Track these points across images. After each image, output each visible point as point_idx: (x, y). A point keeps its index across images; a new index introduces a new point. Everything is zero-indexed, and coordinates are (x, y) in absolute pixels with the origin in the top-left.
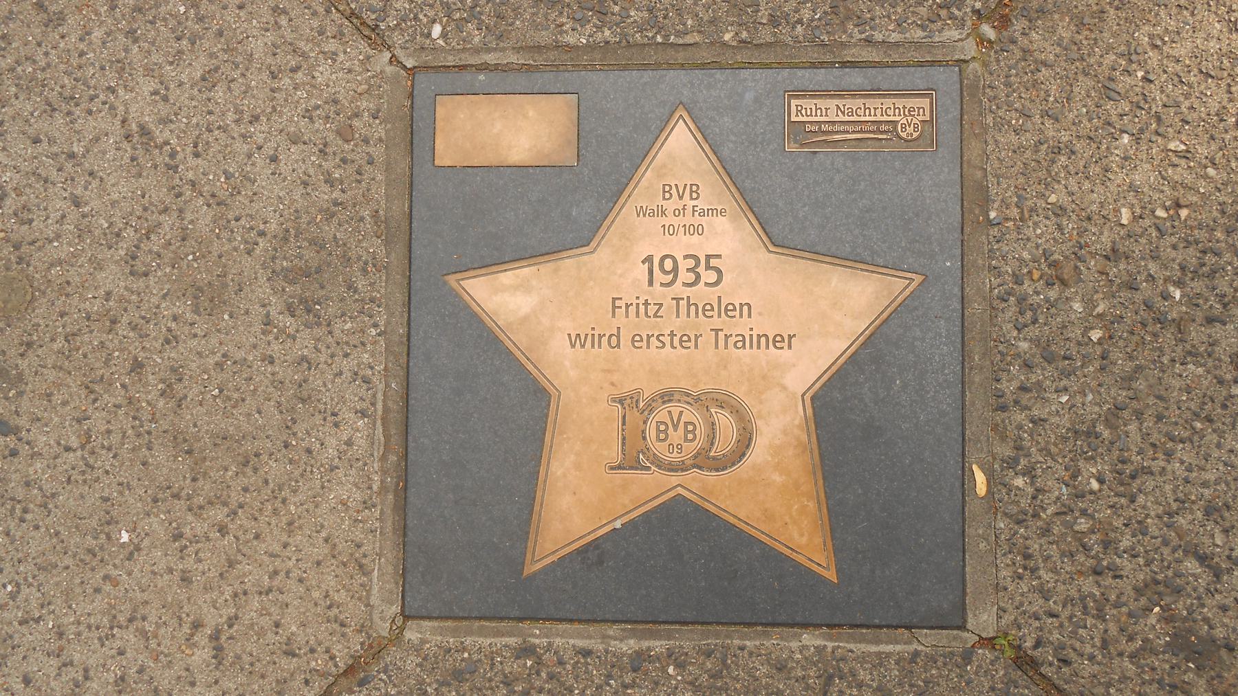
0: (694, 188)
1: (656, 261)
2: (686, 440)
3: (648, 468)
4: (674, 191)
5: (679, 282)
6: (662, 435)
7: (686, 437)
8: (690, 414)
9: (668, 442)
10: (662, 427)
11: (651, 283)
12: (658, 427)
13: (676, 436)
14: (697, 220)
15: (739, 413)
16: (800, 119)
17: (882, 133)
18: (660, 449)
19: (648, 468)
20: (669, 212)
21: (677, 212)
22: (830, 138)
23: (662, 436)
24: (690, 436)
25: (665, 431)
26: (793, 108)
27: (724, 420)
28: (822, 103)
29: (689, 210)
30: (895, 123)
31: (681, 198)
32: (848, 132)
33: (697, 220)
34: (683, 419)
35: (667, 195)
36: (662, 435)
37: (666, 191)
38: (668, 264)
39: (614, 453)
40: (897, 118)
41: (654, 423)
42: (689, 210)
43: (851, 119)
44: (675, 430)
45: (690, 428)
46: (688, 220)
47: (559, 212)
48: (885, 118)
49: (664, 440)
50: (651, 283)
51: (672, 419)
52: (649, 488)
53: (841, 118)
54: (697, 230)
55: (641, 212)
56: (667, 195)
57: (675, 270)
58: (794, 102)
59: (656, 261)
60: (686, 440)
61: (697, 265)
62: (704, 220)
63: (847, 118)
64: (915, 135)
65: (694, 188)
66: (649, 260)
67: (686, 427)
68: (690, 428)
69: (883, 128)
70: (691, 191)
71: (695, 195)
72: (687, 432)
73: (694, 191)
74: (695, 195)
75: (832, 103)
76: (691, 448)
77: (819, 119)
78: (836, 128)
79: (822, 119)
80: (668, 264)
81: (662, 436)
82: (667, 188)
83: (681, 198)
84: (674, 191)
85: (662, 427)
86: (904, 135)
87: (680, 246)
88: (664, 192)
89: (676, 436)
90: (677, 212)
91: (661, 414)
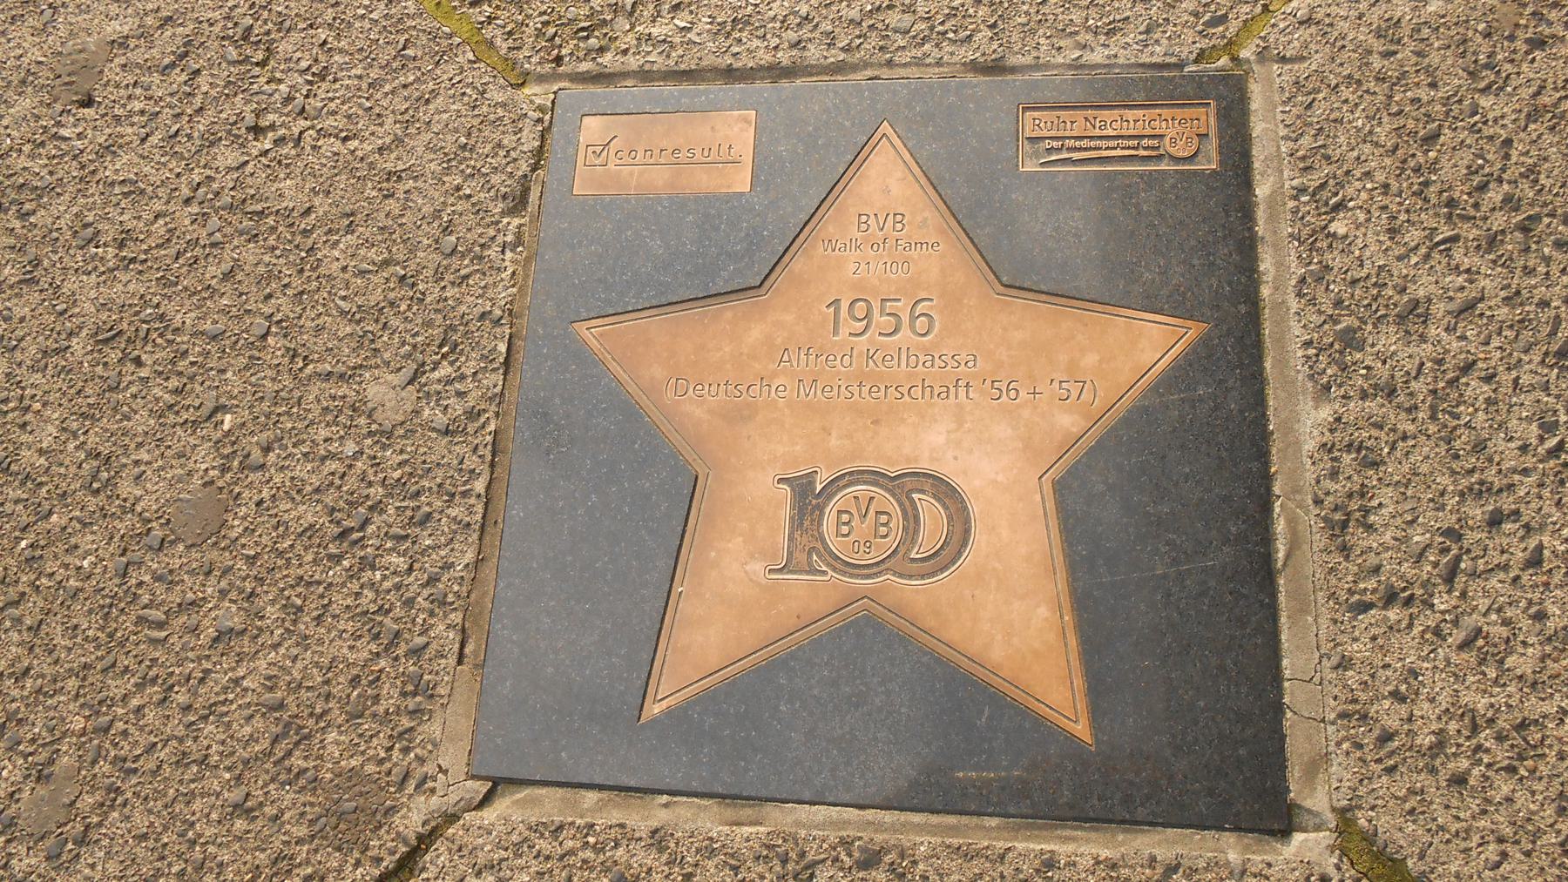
1: (845, 305)
3: (825, 573)
9: (852, 538)
13: (862, 528)
15: (945, 491)
19: (825, 573)
22: (1076, 156)
23: (845, 529)
27: (930, 509)
29: (891, 242)
43: (1105, 133)
51: (859, 509)
59: (845, 305)
63: (1097, 132)
69: (1145, 142)
74: (899, 226)
77: (1060, 134)
78: (1085, 143)
79: (1067, 133)
81: (845, 529)
85: (845, 517)
89: (862, 528)
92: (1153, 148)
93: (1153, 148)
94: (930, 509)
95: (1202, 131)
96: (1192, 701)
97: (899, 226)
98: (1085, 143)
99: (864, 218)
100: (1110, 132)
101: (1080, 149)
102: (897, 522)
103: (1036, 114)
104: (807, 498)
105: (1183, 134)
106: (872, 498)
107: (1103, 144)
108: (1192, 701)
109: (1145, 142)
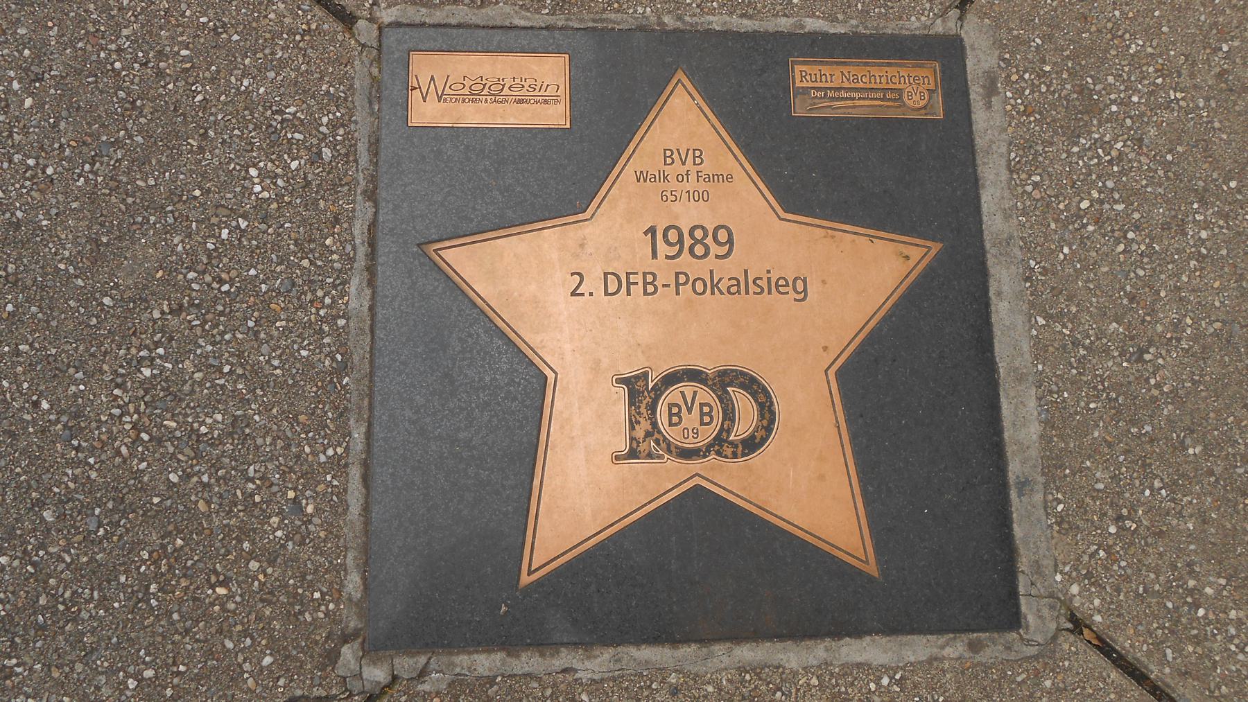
0: (698, 153)
2: (702, 424)
4: (675, 156)
6: (675, 416)
7: (701, 419)
8: (705, 395)
10: (675, 410)
11: (654, 255)
12: (670, 410)
13: (691, 420)
14: (702, 186)
16: (805, 84)
17: (889, 100)
18: (673, 434)
21: (680, 178)
24: (707, 419)
25: (678, 414)
28: (826, 70)
29: (693, 177)
30: (900, 91)
31: (684, 164)
32: (853, 99)
35: (669, 161)
36: (675, 416)
37: (668, 155)
40: (900, 86)
41: (665, 408)
42: (693, 177)
44: (690, 410)
45: (706, 409)
47: (553, 178)
49: (676, 425)
50: (654, 255)
52: (663, 479)
53: (846, 85)
54: (703, 197)
55: (641, 177)
56: (669, 161)
57: (681, 241)
58: (798, 68)
60: (702, 424)
61: (706, 235)
64: (922, 103)
65: (698, 153)
66: (652, 231)
67: (701, 410)
68: (706, 409)
70: (694, 157)
71: (698, 161)
72: (702, 414)
73: (697, 155)
78: (843, 94)
81: (675, 419)
82: (668, 153)
83: (684, 164)
84: (675, 156)
85: (675, 410)
86: (910, 103)
87: (688, 215)
88: (665, 157)
89: (691, 420)
90: (680, 178)
91: (672, 395)
92: (895, 100)
93: (895, 100)
94: (744, 404)
95: (932, 87)
96: (946, 543)
97: (698, 161)
98: (843, 94)
99: (668, 153)
100: (861, 85)
101: (839, 99)
102: (718, 415)
103: (804, 68)
105: (916, 89)
106: (695, 393)
107: (856, 95)
108: (946, 543)
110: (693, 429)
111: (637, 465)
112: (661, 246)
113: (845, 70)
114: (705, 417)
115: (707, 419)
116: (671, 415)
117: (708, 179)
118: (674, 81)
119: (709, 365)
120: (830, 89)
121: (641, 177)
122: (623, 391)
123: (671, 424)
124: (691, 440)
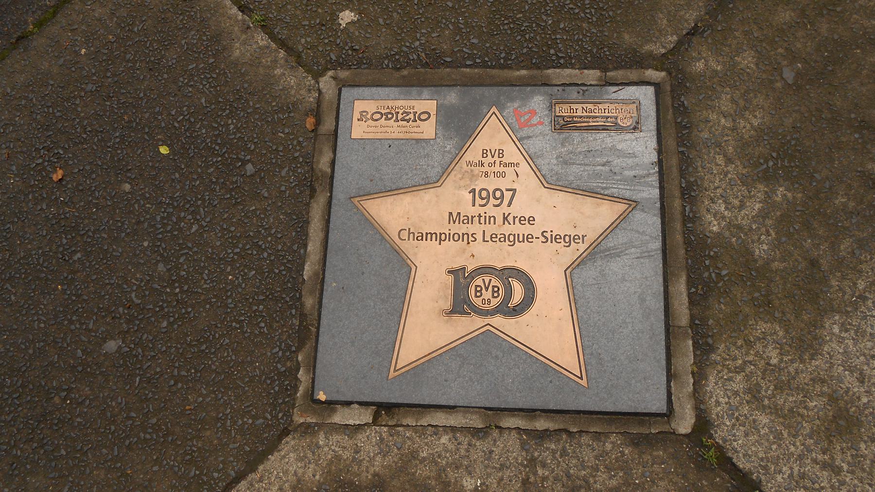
2: (494, 297)
4: (489, 153)
5: (490, 205)
6: (478, 292)
13: (487, 295)
14: (502, 169)
16: (561, 114)
18: (478, 302)
20: (486, 165)
23: (478, 294)
24: (496, 295)
26: (557, 109)
29: (498, 163)
33: (502, 169)
34: (492, 284)
37: (484, 153)
38: (484, 194)
39: (447, 305)
42: (498, 163)
44: (487, 289)
46: (497, 168)
48: (610, 114)
53: (585, 114)
54: (503, 175)
62: (505, 169)
68: (496, 289)
72: (493, 292)
73: (501, 153)
75: (579, 106)
76: (495, 302)
79: (575, 114)
80: (484, 194)
81: (478, 294)
84: (489, 153)
85: (479, 289)
87: (491, 184)
89: (487, 295)
91: (479, 282)
100: (593, 114)
104: (461, 278)
107: (591, 120)
109: (609, 120)
110: (488, 299)
111: (456, 318)
112: (478, 201)
113: (584, 106)
114: (495, 291)
115: (496, 295)
116: (476, 291)
117: (506, 165)
118: (491, 112)
119: (499, 265)
120: (575, 117)
121: (469, 163)
122: (451, 278)
123: (476, 296)
124: (486, 305)
